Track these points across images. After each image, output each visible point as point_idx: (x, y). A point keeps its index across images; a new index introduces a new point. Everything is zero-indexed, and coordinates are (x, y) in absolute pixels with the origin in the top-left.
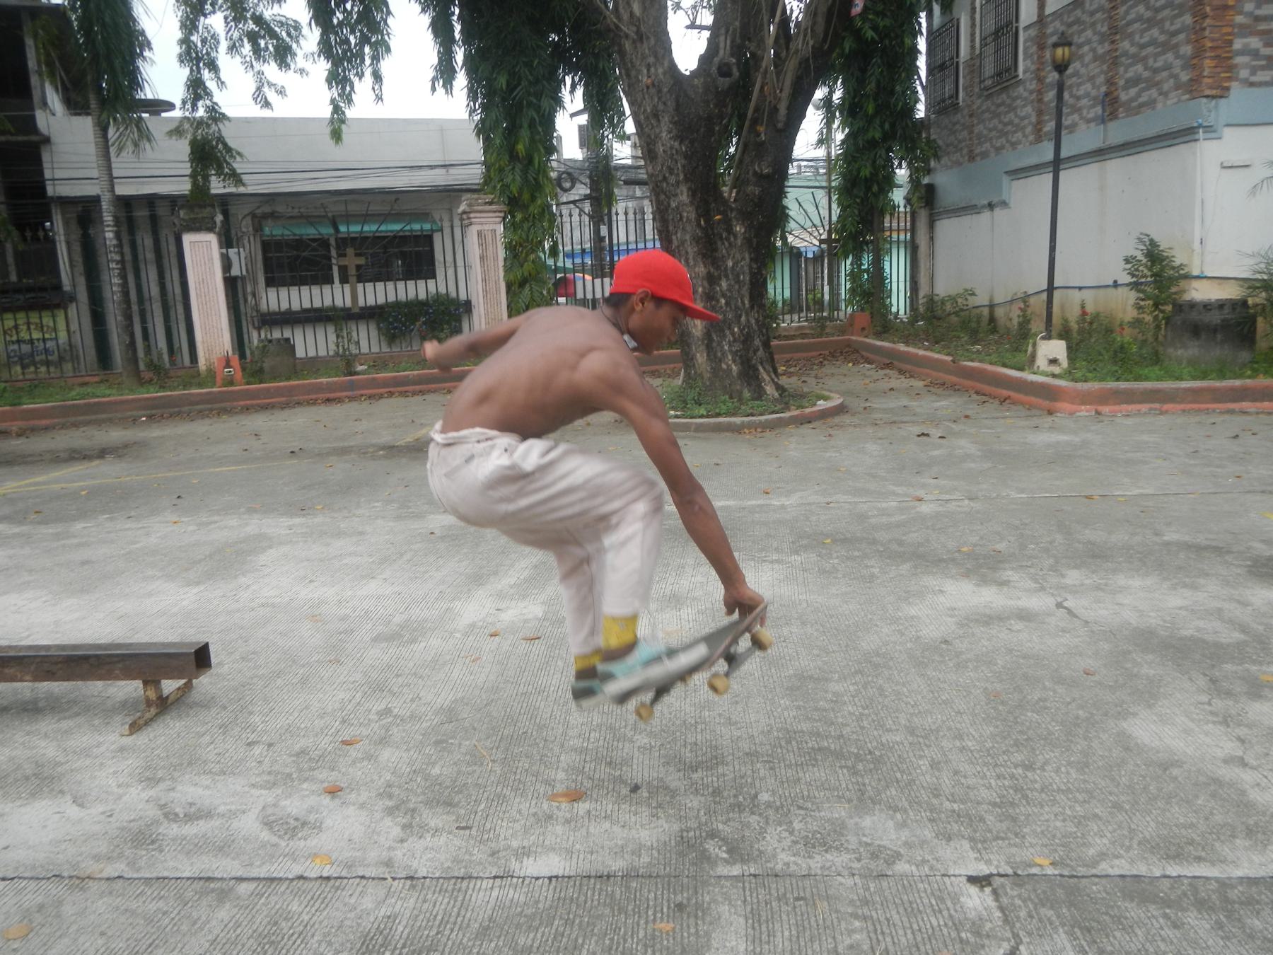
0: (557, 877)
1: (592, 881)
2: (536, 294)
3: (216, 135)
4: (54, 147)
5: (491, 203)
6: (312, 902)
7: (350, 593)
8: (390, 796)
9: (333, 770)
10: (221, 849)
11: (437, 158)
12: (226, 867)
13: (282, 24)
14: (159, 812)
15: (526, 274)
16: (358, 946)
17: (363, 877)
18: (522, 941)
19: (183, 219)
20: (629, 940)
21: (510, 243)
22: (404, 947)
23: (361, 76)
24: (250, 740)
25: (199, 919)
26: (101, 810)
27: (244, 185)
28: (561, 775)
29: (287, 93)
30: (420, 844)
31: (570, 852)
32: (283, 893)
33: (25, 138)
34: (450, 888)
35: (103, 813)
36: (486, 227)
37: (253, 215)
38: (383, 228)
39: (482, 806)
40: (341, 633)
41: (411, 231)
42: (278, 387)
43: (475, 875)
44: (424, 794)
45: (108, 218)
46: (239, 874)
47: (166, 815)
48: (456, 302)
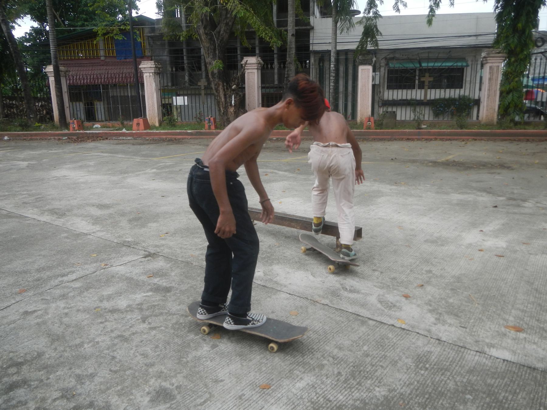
0: (507, 361)
1: (526, 368)
2: (515, 98)
4: (315, 31)
5: (499, 53)
6: (397, 336)
7: (415, 220)
8: (430, 305)
9: (406, 288)
10: (362, 306)
11: (472, 32)
12: (364, 312)
14: (340, 286)
15: (512, 88)
16: (415, 358)
17: (418, 333)
18: (489, 381)
20: (544, 399)
22: (435, 365)
25: (355, 328)
26: (321, 280)
28: (511, 318)
30: (443, 328)
31: (514, 352)
32: (386, 329)
33: (305, 27)
34: (456, 349)
35: (321, 281)
36: (494, 65)
37: (386, 58)
38: (444, 64)
39: (472, 321)
40: (411, 236)
41: (457, 66)
42: (388, 132)
43: (468, 347)
44: (446, 309)
45: (333, 59)
46: (369, 317)
47: (343, 288)
48: (469, 99)
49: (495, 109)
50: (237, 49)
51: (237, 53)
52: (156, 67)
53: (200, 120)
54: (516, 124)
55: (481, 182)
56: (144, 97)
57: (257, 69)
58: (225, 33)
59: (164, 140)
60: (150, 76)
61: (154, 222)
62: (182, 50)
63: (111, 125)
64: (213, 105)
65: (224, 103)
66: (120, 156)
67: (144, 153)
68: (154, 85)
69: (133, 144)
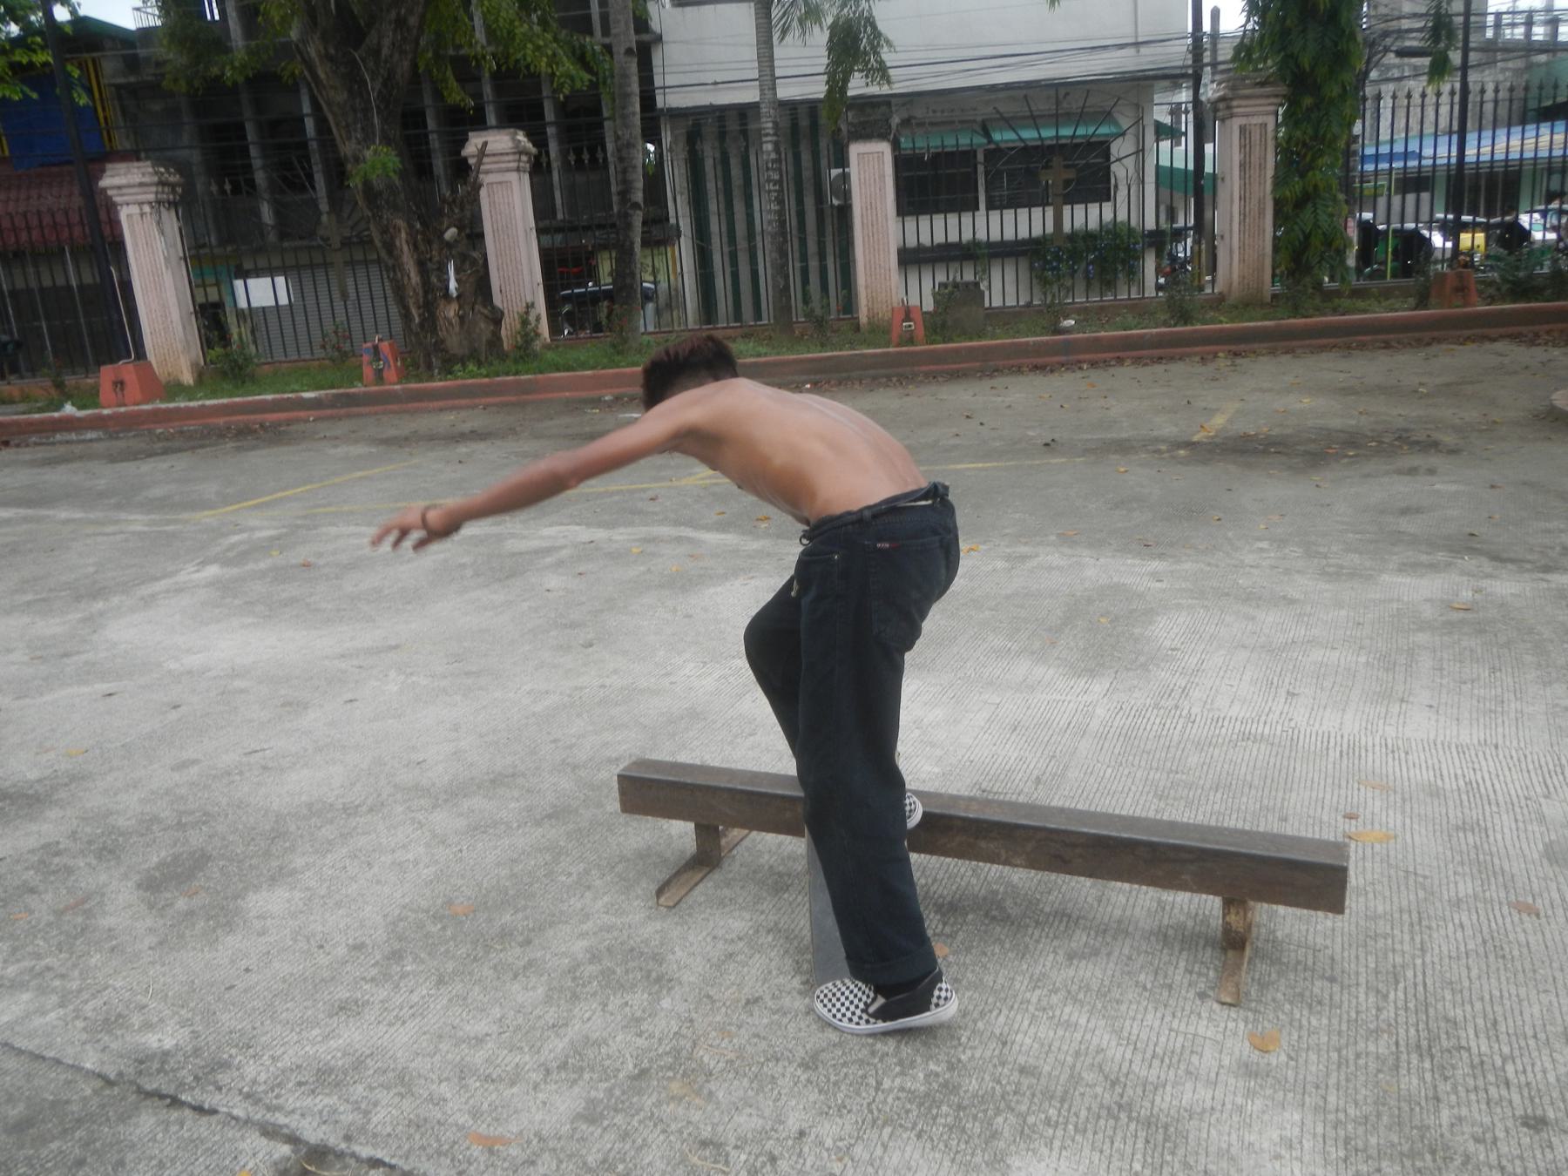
2: (1323, 217)
5: (1262, 84)
15: (1310, 189)
19: (852, 124)
21: (1289, 139)
24: (1519, 1112)
27: (889, 82)
48: (1131, 231)
49: (1264, 255)
50: (423, 114)
51: (425, 126)
52: (161, 183)
54: (1329, 296)
56: (127, 287)
57: (518, 170)
58: (396, 57)
59: (222, 434)
60: (142, 215)
61: (273, 879)
62: (241, 128)
63: (16, 393)
64: (380, 303)
65: (421, 293)
66: (63, 514)
67: (157, 492)
68: (159, 244)
69: (113, 459)
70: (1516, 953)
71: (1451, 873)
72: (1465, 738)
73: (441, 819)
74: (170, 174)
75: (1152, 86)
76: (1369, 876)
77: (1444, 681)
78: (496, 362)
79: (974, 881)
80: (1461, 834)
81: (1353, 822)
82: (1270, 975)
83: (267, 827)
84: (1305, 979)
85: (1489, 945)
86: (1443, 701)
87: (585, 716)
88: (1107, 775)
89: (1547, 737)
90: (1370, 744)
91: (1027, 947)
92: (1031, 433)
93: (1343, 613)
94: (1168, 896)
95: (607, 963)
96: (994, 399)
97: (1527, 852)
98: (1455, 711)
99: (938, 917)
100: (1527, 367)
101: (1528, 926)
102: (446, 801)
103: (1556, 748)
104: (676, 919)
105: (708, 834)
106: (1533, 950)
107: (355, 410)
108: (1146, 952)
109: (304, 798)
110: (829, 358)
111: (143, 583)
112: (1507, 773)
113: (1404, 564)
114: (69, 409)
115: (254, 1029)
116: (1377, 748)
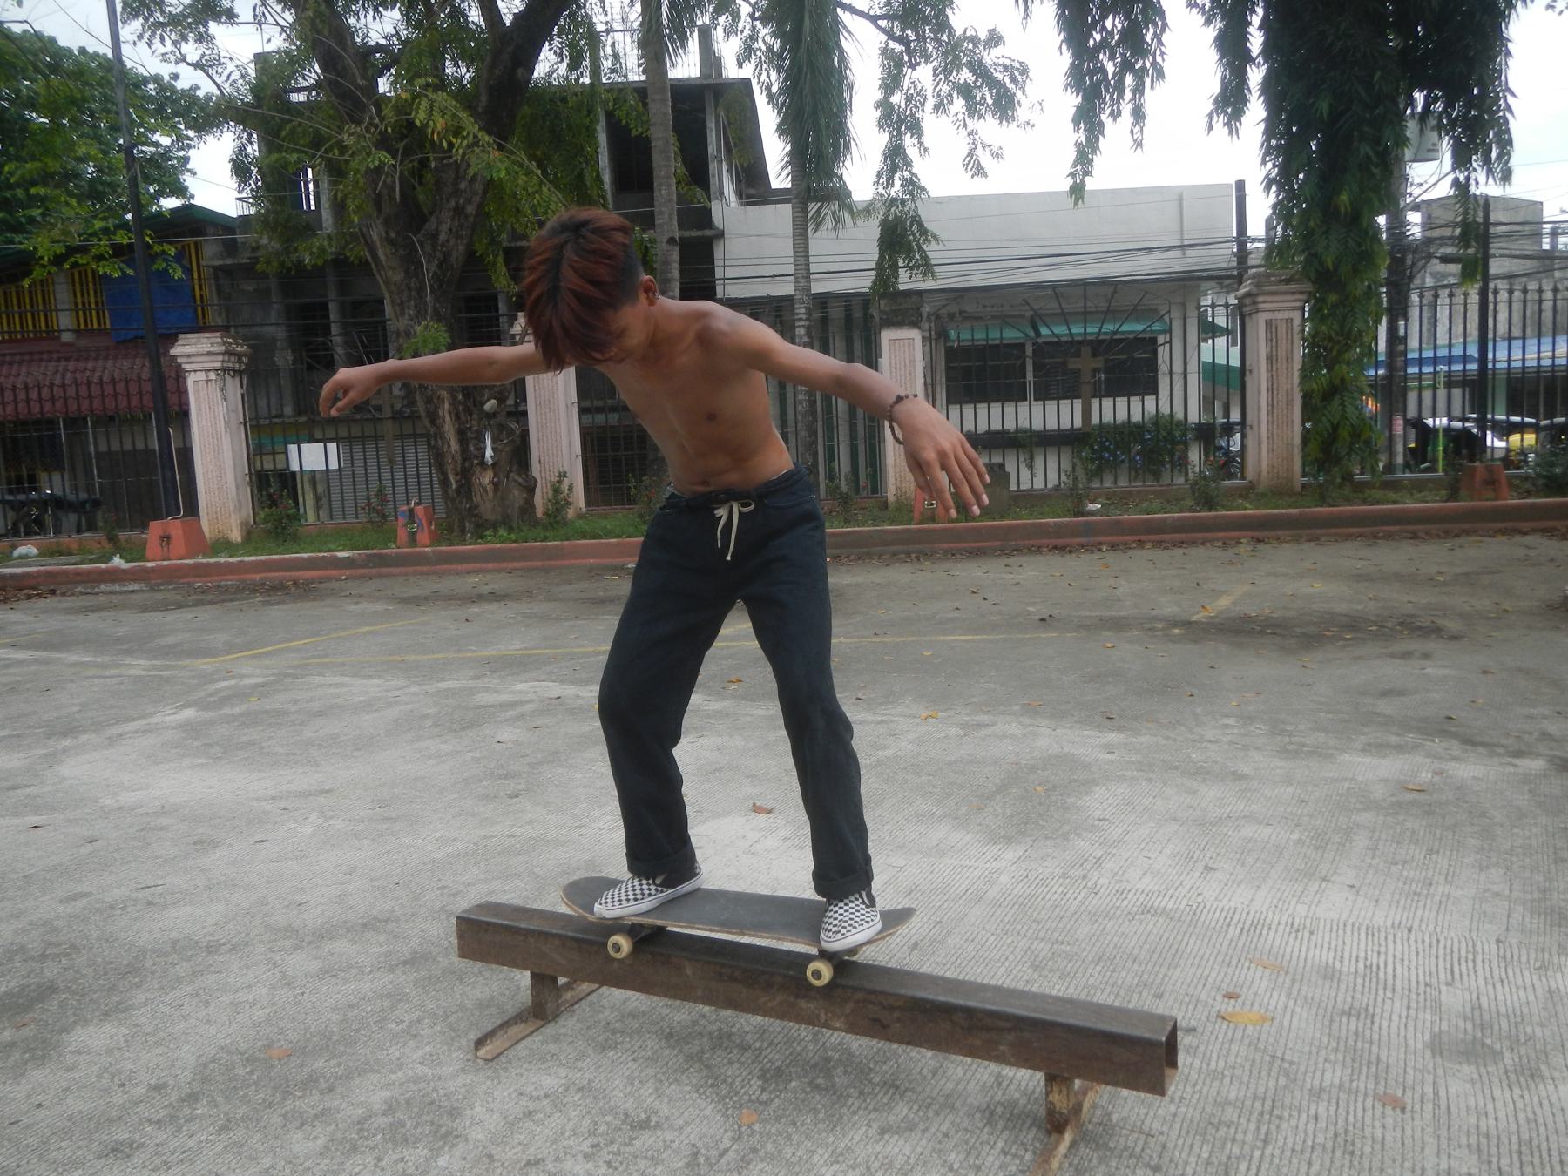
2: (1350, 409)
3: (912, 213)
5: (1287, 281)
7: (1301, 910)
13: (1005, 68)
15: (1337, 382)
21: (1314, 335)
23: (1115, 115)
27: (935, 279)
29: (1005, 153)
33: (699, 233)
36: (1280, 315)
40: (1349, 1015)
49: (1292, 445)
50: (496, 299)
51: (497, 310)
52: (227, 353)
53: (379, 518)
54: (1360, 487)
55: (1401, 693)
58: (452, 241)
59: (254, 589)
60: (208, 381)
61: (106, 1014)
62: (325, 307)
63: (74, 546)
64: (424, 470)
65: (459, 458)
66: (74, 658)
67: (170, 640)
68: (221, 409)
69: (144, 609)
70: (1367, 1149)
71: (1321, 1060)
72: (1379, 920)
73: (301, 962)
74: (237, 344)
75: (1199, 286)
76: (1232, 1059)
77: (1374, 862)
78: (525, 529)
79: (810, 1046)
80: (1344, 1020)
81: (1232, 1001)
82: (1090, 1161)
83: (125, 962)
84: (1128, 1167)
85: (1340, 1140)
86: (1367, 881)
87: (482, 864)
88: (988, 943)
89: (1467, 922)
90: (1276, 922)
91: (841, 1118)
92: (1031, 609)
93: (1290, 790)
94: (1008, 1071)
95: (400, 1115)
96: (1003, 575)
97: (1411, 1042)
98: (1377, 892)
99: (760, 1083)
100: (1552, 560)
101: (1389, 1121)
102: (310, 943)
103: (1474, 935)
104: (490, 1073)
105: (542, 981)
106: (1387, 1146)
107: (385, 570)
108: (966, 1130)
109: (174, 935)
110: (849, 533)
111: (117, 723)
112: (1413, 957)
113: (1369, 745)
114: (117, 561)
115: (18, 1166)
116: (1281, 927)
